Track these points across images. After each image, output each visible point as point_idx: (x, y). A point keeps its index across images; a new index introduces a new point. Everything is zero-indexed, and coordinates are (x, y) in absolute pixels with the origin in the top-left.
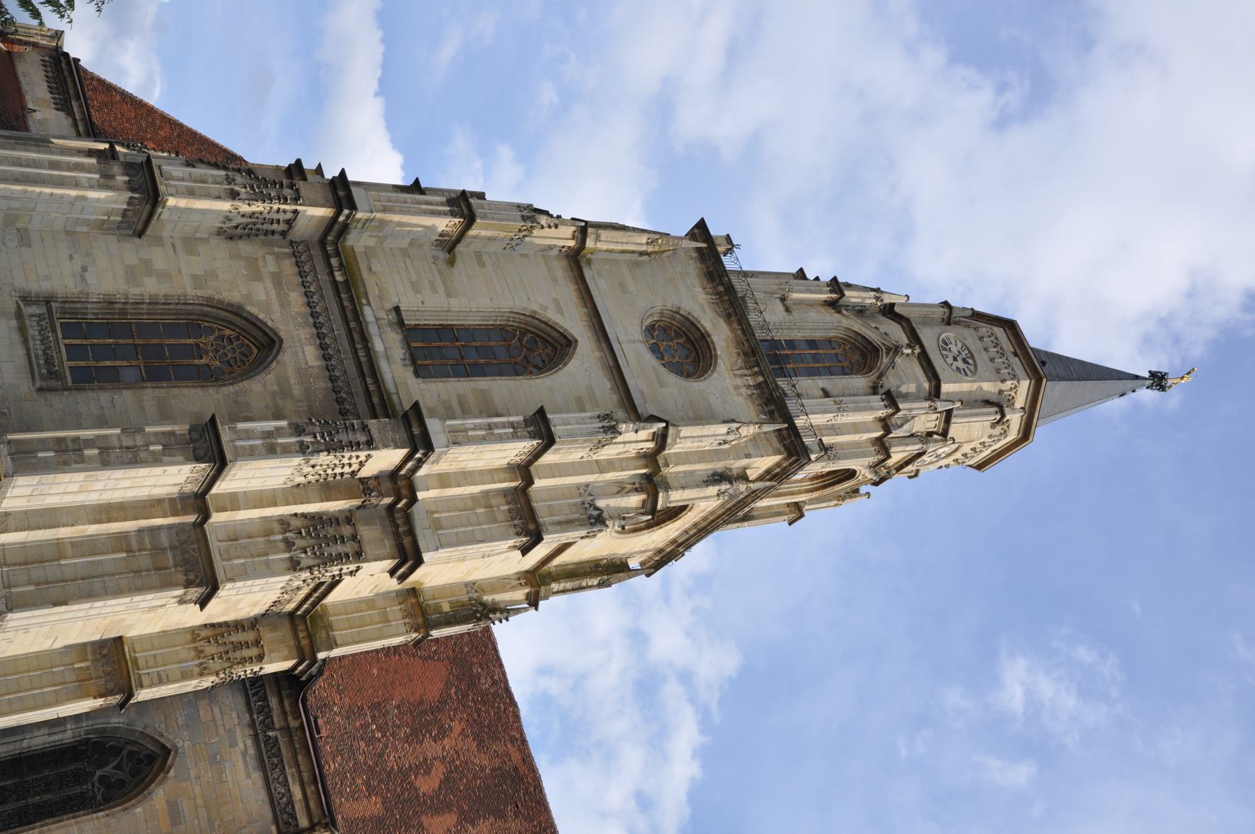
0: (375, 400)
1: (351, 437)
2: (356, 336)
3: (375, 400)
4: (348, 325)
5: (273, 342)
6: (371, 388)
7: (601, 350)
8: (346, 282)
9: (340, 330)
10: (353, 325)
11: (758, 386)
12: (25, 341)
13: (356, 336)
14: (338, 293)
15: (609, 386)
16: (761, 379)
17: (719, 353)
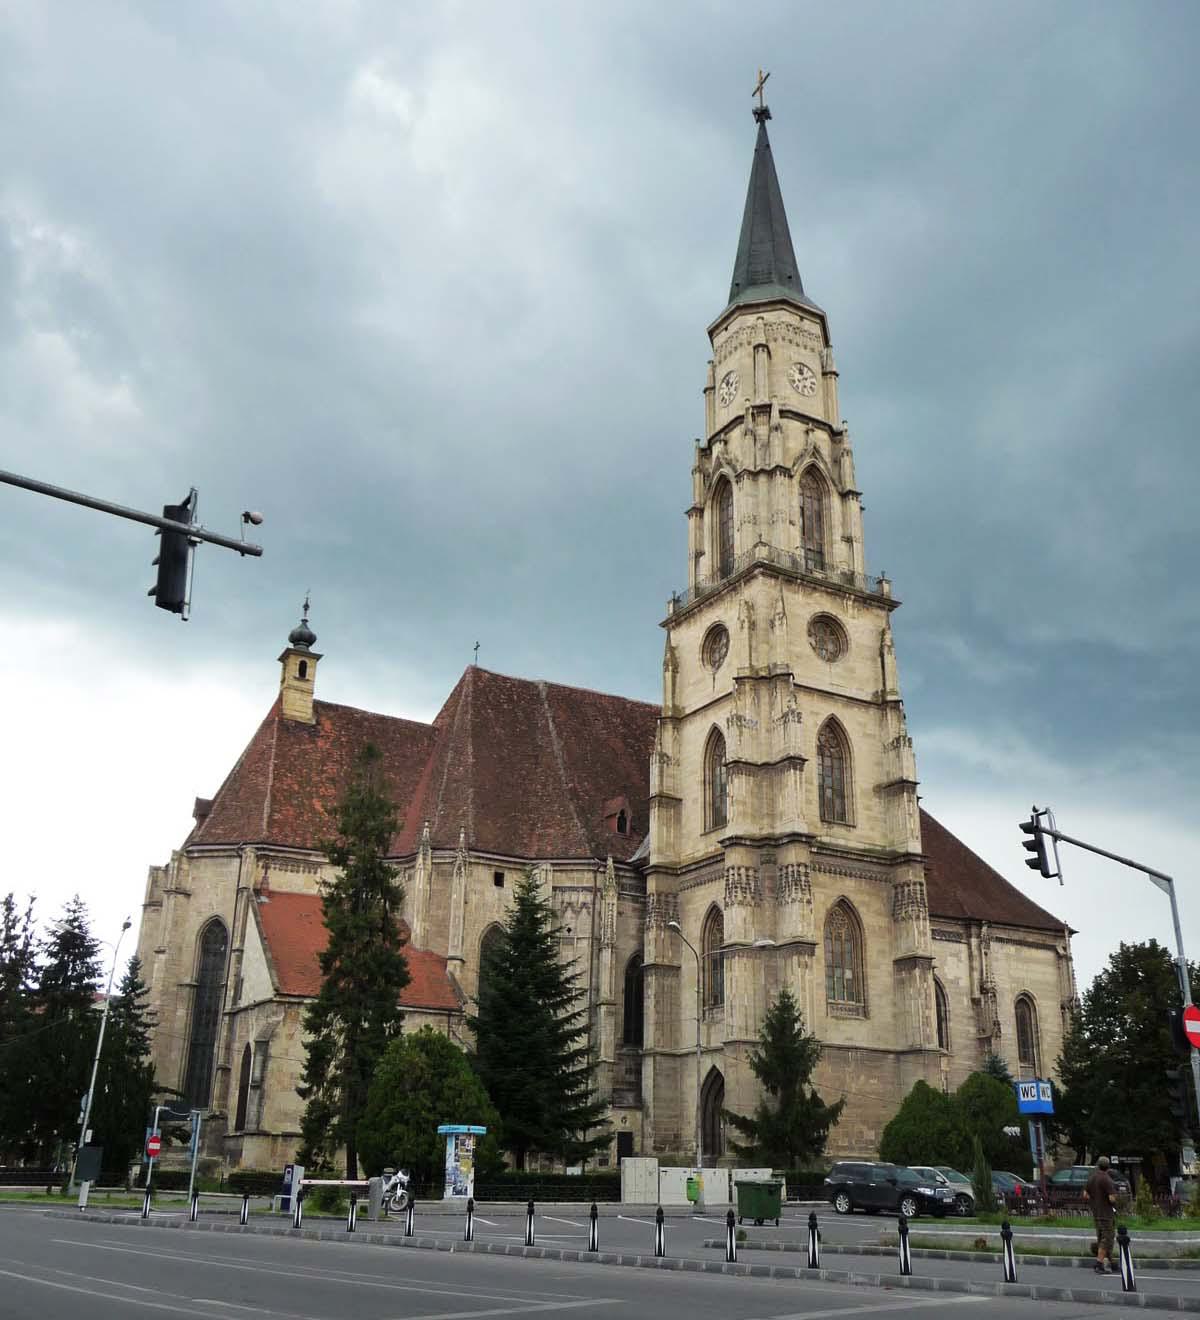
0: (875, 860)
1: (919, 892)
2: (845, 855)
3: (875, 860)
4: (837, 856)
5: (842, 900)
6: (869, 859)
7: (836, 701)
8: (819, 848)
9: (839, 861)
10: (839, 854)
11: (855, 601)
12: (850, 1019)
13: (845, 855)
14: (821, 854)
15: (856, 709)
16: (853, 597)
17: (834, 614)
